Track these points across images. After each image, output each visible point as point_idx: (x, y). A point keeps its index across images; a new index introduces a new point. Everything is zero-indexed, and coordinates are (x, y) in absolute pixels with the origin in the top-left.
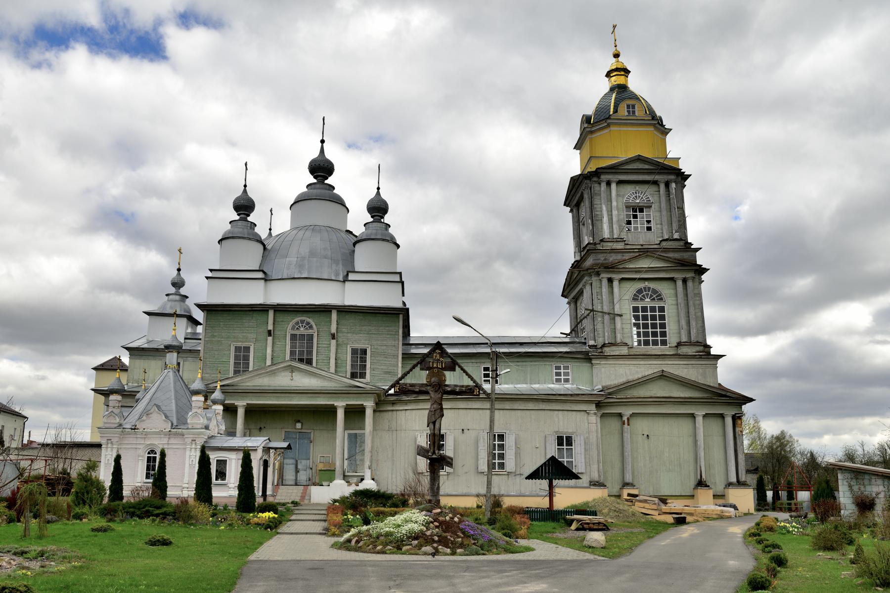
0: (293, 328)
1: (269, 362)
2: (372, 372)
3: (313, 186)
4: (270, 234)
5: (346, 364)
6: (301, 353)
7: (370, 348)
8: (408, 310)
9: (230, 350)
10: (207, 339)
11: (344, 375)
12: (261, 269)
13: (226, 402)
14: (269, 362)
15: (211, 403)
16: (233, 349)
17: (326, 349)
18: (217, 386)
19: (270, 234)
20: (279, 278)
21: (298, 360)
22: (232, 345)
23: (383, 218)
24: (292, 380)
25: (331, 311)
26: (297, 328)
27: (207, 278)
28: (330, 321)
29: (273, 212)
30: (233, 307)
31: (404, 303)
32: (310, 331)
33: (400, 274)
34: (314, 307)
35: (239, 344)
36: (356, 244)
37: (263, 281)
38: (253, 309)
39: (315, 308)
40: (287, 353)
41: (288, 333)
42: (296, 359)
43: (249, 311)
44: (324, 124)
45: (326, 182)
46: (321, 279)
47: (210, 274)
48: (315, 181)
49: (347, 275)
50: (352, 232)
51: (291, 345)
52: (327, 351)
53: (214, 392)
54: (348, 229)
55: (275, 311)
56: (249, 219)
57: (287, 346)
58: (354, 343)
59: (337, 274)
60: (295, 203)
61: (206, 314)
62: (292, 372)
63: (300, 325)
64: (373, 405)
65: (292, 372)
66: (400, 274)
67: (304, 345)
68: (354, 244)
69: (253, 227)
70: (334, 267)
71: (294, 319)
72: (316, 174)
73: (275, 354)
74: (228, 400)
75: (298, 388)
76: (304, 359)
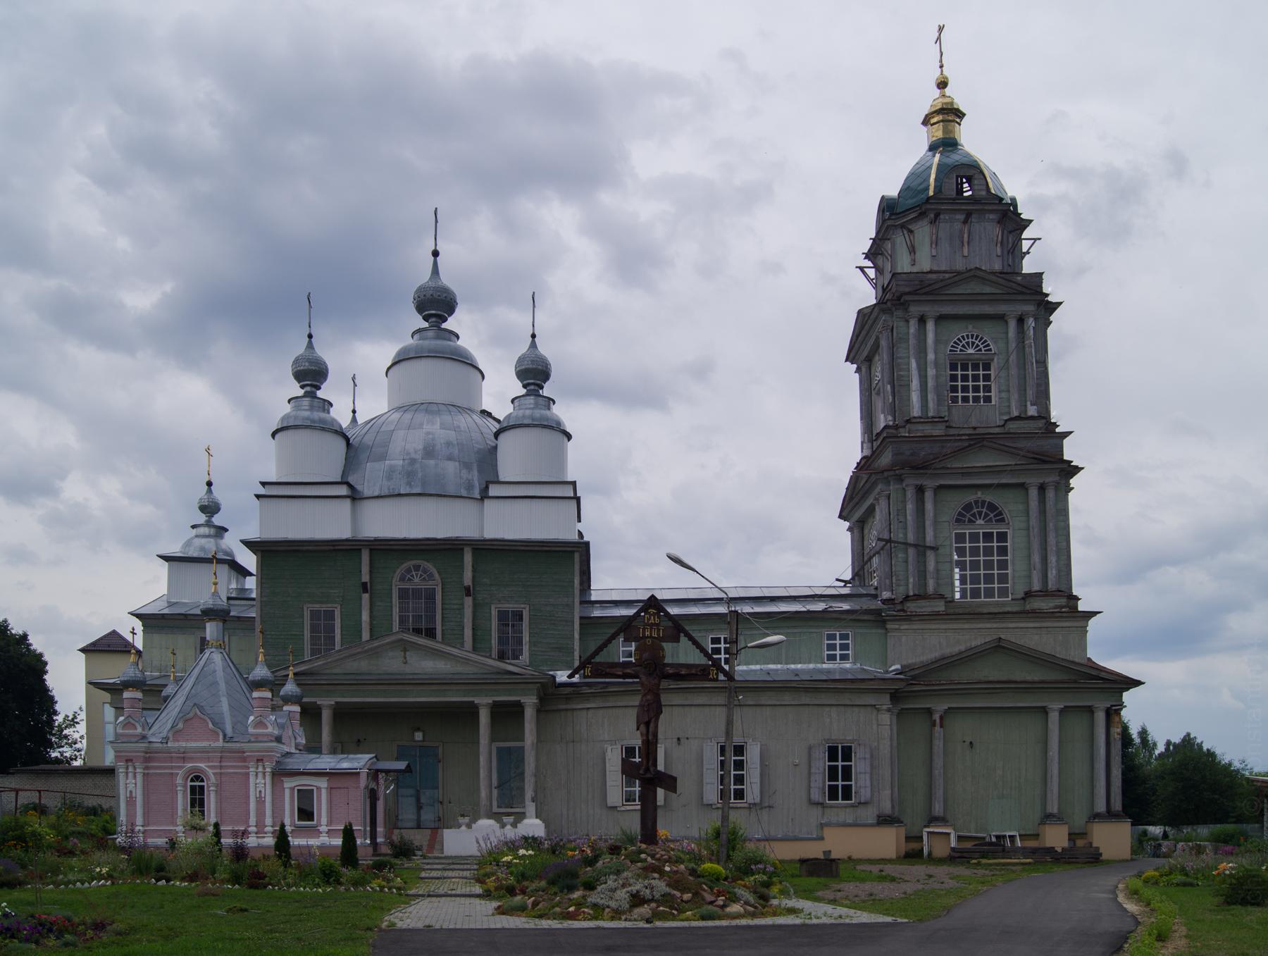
0: (402, 579)
1: (366, 635)
2: (533, 649)
3: (425, 333)
4: (354, 420)
5: (491, 635)
6: (417, 618)
7: (528, 609)
8: (587, 544)
9: (302, 616)
10: (265, 599)
11: (488, 654)
12: (345, 480)
13: (305, 700)
14: (366, 635)
15: (281, 702)
16: (307, 615)
17: (457, 612)
18: (288, 675)
19: (354, 420)
20: (376, 494)
21: (413, 631)
22: (305, 608)
23: (542, 388)
24: (406, 663)
25: (462, 549)
26: (409, 580)
27: (258, 496)
28: (462, 567)
29: (356, 381)
30: (303, 546)
31: (580, 534)
32: (431, 582)
33: (574, 484)
34: (435, 542)
35: (317, 607)
36: (498, 435)
37: (348, 501)
38: (336, 548)
39: (437, 545)
40: (394, 619)
41: (394, 587)
42: (409, 630)
43: (330, 551)
44: (436, 221)
45: (444, 326)
46: (445, 496)
47: (262, 491)
48: (426, 325)
49: (487, 487)
50: (491, 414)
51: (399, 607)
52: (459, 616)
53: (285, 684)
54: (484, 408)
55: (371, 550)
56: (320, 394)
57: (394, 609)
58: (502, 602)
59: (470, 487)
60: (394, 364)
61: (260, 557)
62: (405, 650)
63: (414, 573)
64: (536, 701)
65: (405, 650)
66: (574, 484)
67: (422, 607)
68: (497, 435)
69: (326, 407)
70: (465, 474)
71: (402, 563)
72: (427, 313)
73: (374, 622)
74: (306, 697)
75: (415, 677)
76: (422, 629)
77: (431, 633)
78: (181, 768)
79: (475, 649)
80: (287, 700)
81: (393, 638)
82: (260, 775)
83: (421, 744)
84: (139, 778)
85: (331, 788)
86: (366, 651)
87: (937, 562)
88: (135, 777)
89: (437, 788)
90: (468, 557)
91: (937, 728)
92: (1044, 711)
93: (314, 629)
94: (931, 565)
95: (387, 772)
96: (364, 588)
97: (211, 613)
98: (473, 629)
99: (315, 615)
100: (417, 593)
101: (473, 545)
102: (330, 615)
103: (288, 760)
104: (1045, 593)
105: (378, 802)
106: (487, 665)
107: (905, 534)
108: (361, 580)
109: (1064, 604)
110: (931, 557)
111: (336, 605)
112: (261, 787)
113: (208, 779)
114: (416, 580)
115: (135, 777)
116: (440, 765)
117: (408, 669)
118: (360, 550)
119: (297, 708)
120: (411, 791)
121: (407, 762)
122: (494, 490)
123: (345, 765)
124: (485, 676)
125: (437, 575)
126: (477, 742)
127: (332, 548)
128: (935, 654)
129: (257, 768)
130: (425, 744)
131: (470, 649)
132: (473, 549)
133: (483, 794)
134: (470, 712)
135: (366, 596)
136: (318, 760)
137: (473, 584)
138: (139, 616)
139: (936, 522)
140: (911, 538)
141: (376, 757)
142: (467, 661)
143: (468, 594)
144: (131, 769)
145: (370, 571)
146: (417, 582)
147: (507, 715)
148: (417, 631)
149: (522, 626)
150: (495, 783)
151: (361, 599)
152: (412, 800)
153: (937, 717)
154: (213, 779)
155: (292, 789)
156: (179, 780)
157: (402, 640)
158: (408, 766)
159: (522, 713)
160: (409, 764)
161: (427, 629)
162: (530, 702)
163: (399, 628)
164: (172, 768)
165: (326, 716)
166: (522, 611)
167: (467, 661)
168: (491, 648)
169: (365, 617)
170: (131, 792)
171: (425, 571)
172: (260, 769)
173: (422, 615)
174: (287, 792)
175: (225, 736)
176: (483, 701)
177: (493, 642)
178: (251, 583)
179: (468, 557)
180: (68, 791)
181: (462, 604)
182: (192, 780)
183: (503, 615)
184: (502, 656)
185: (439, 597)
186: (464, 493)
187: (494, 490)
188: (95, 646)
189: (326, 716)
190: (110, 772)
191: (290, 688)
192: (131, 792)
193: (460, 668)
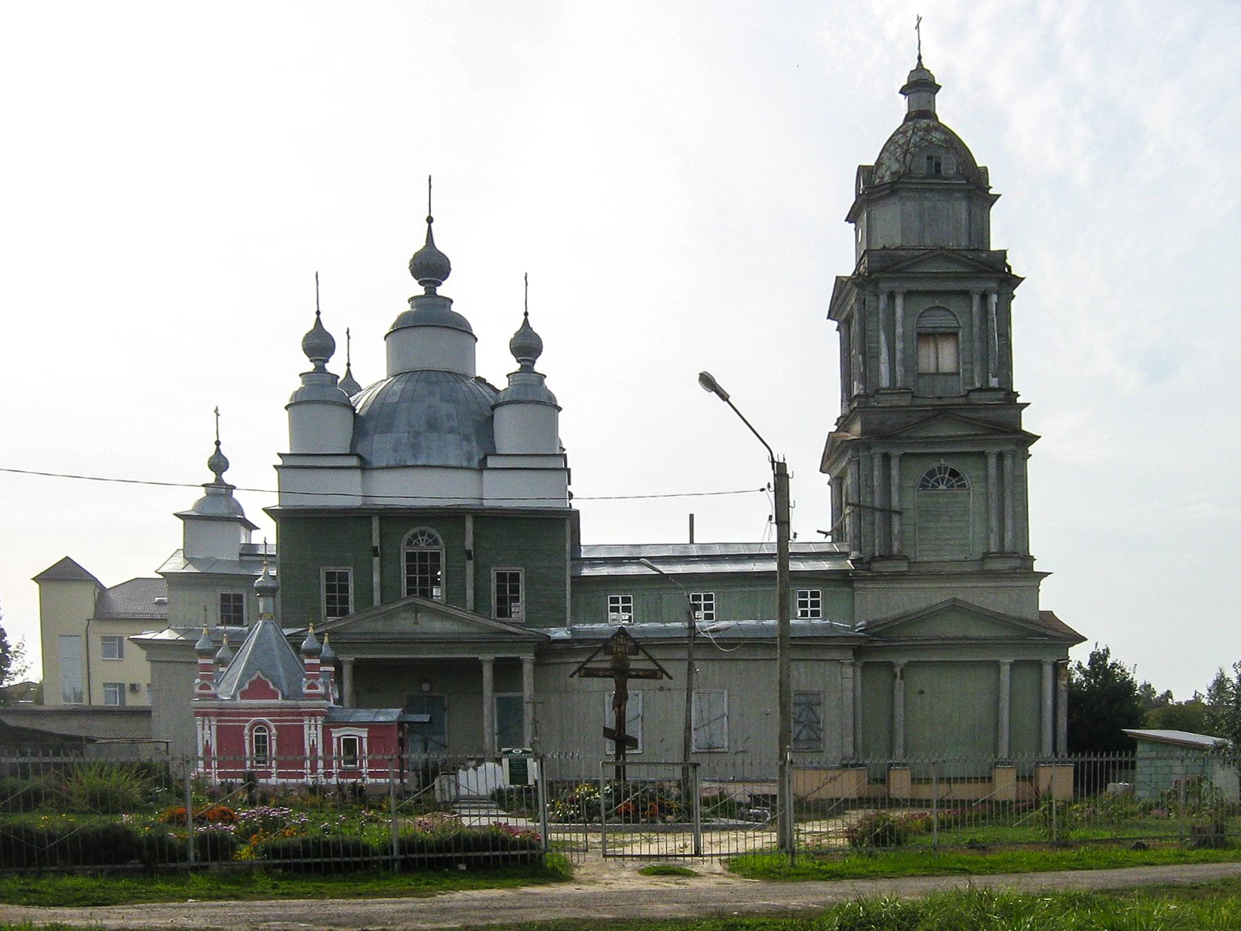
78: (247, 721)
79: (476, 611)
84: (214, 728)
87: (902, 525)
88: (210, 729)
91: (898, 680)
92: (996, 665)
94: (896, 528)
104: (1002, 554)
107: (873, 500)
109: (1018, 565)
110: (896, 520)
113: (270, 731)
115: (210, 729)
122: (491, 462)
128: (898, 612)
134: (477, 666)
139: (900, 487)
140: (877, 504)
142: (470, 623)
144: (207, 722)
147: (508, 671)
153: (898, 670)
156: (246, 731)
159: (521, 666)
162: (528, 658)
164: (240, 721)
167: (470, 623)
170: (207, 741)
176: (487, 657)
182: (256, 732)
186: (465, 464)
187: (491, 462)
192: (207, 741)
193: (464, 629)
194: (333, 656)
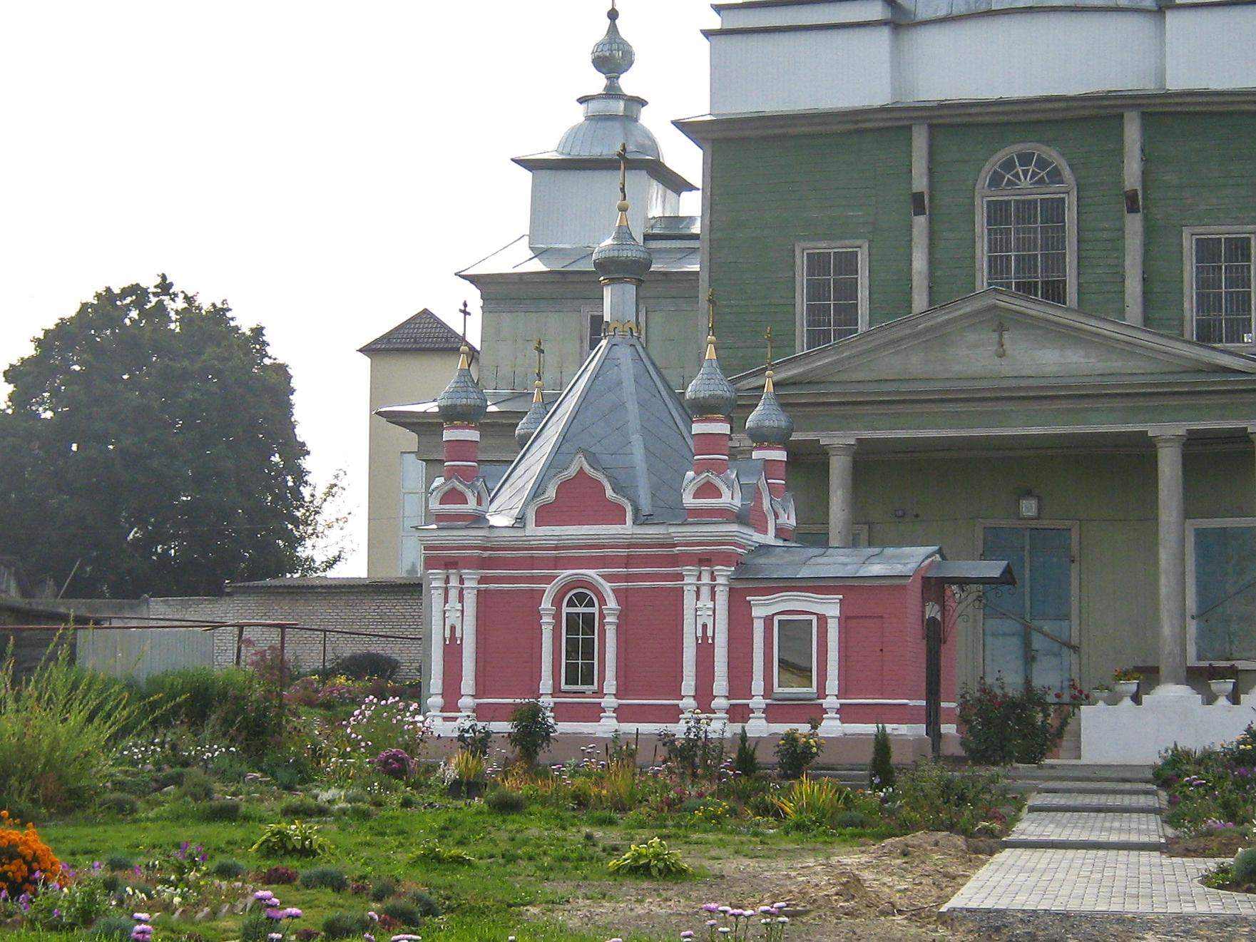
0: (995, 181)
1: (920, 301)
6: (1026, 263)
13: (795, 437)
14: (920, 301)
15: (748, 443)
16: (801, 262)
21: (1018, 288)
22: (798, 251)
25: (1121, 116)
28: (1119, 152)
34: (1063, 105)
35: (822, 246)
40: (977, 266)
41: (977, 200)
42: (1008, 286)
51: (990, 241)
55: (931, 127)
57: (978, 245)
62: (1001, 329)
63: (1020, 169)
65: (1001, 329)
67: (1035, 238)
71: (996, 151)
75: (1023, 383)
76: (1036, 283)
77: (1054, 293)
78: (549, 579)
80: (762, 438)
81: (977, 305)
82: (705, 592)
83: (1034, 524)
84: (470, 599)
85: (847, 618)
86: (919, 334)
88: (461, 600)
89: (1067, 617)
90: (1132, 132)
93: (816, 291)
95: (963, 582)
96: (918, 204)
97: (612, 269)
98: (1144, 279)
99: (817, 263)
100: (1026, 209)
101: (1139, 105)
102: (847, 263)
103: (761, 561)
105: (943, 646)
106: (1174, 355)
108: (911, 188)
111: (858, 242)
112: (705, 618)
113: (603, 601)
114: (1025, 183)
115: (461, 600)
116: (1074, 569)
117: (1006, 368)
118: (910, 128)
119: (781, 455)
120: (1010, 625)
121: (1006, 562)
123: (876, 569)
124: (1171, 378)
125: (1067, 172)
126: (1150, 518)
127: (852, 127)
129: (699, 578)
130: (1045, 523)
131: (1139, 324)
132: (1143, 113)
133: (1167, 629)
135: (920, 222)
136: (821, 560)
137: (1144, 188)
138: (474, 279)
141: (940, 552)
142: (1129, 349)
143: (1133, 209)
144: (454, 582)
145: (930, 170)
146: (1026, 187)
148: (1026, 289)
149: (1249, 272)
150: (1191, 604)
151: (910, 227)
152: (1014, 644)
154: (612, 603)
155: (768, 620)
156: (546, 604)
157: (995, 307)
158: (1008, 571)
160: (1008, 565)
161: (1047, 282)
163: (990, 284)
164: (532, 579)
165: (839, 467)
166: (1248, 239)
167: (1129, 349)
168: (1182, 320)
169: (919, 263)
170: (453, 628)
171: (1042, 164)
172: (706, 579)
173: (1036, 255)
174: (758, 627)
175: (636, 511)
177: (1186, 305)
178: (691, 205)
179: (1132, 132)
180: (331, 628)
181: (1122, 230)
182: (571, 604)
183: (1207, 249)
184: (1206, 335)
185: (1071, 217)
188: (389, 342)
189: (839, 467)
190: (412, 589)
191: (761, 415)
192: (453, 628)
194: (783, 424)
